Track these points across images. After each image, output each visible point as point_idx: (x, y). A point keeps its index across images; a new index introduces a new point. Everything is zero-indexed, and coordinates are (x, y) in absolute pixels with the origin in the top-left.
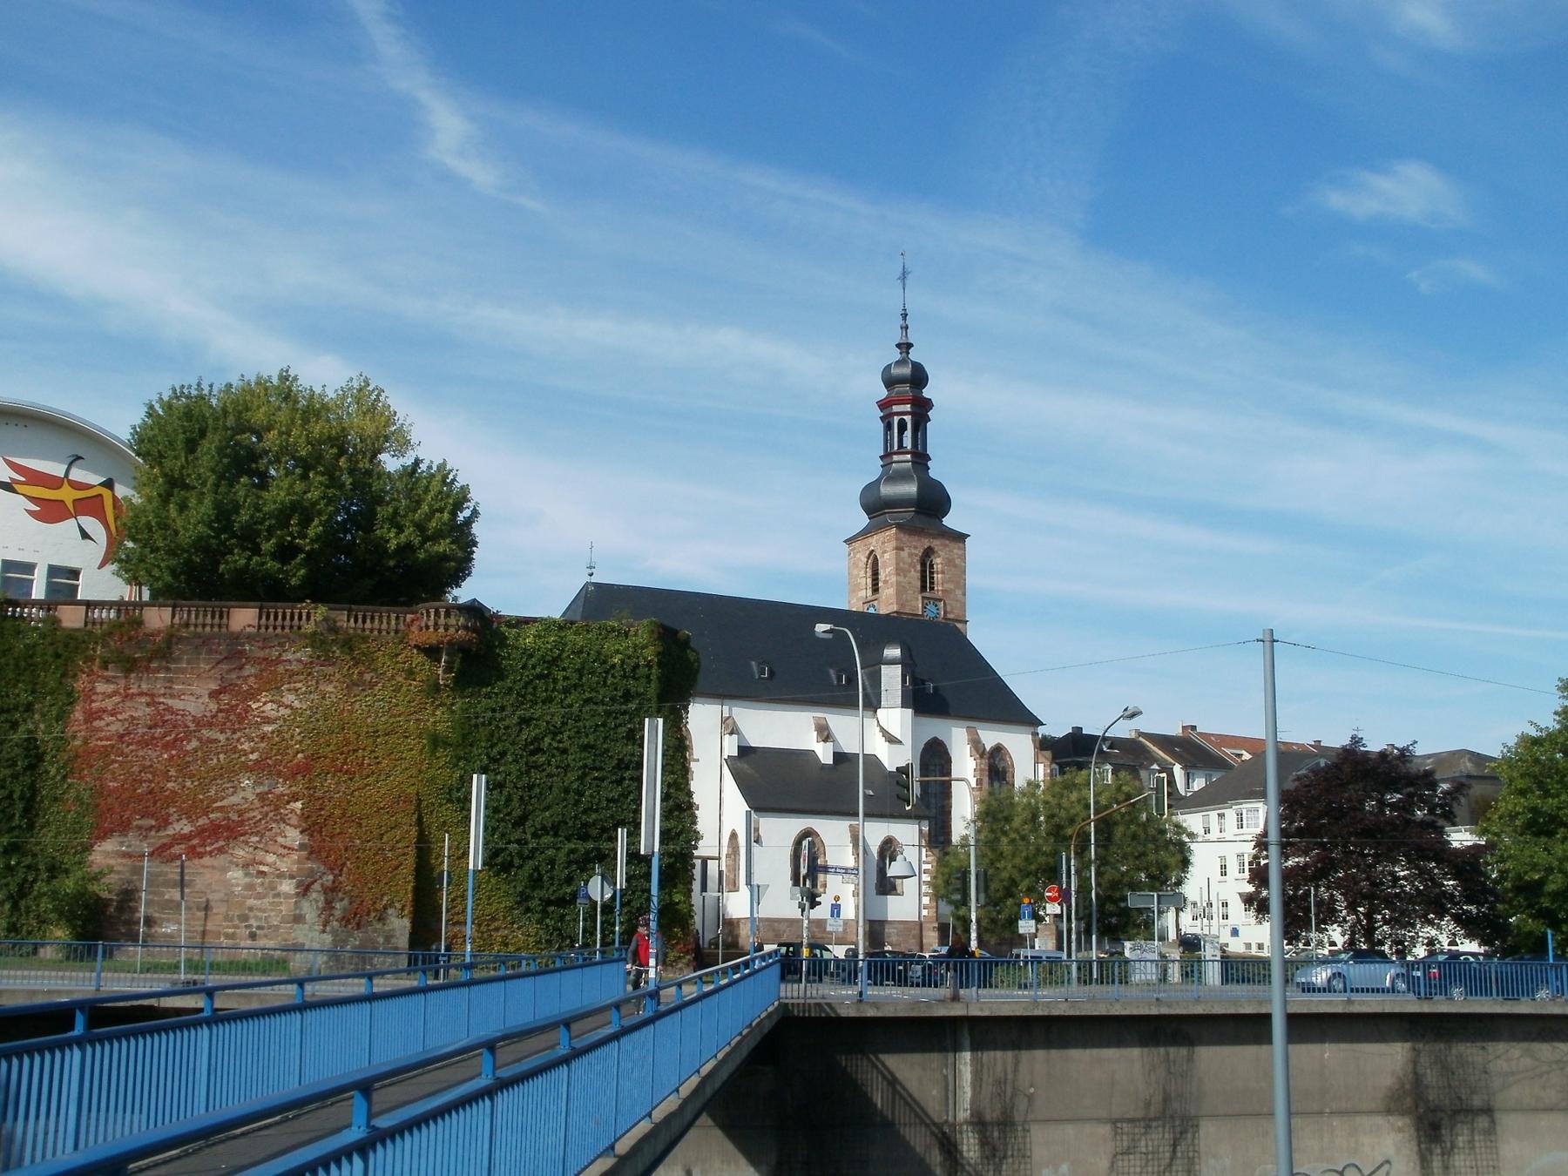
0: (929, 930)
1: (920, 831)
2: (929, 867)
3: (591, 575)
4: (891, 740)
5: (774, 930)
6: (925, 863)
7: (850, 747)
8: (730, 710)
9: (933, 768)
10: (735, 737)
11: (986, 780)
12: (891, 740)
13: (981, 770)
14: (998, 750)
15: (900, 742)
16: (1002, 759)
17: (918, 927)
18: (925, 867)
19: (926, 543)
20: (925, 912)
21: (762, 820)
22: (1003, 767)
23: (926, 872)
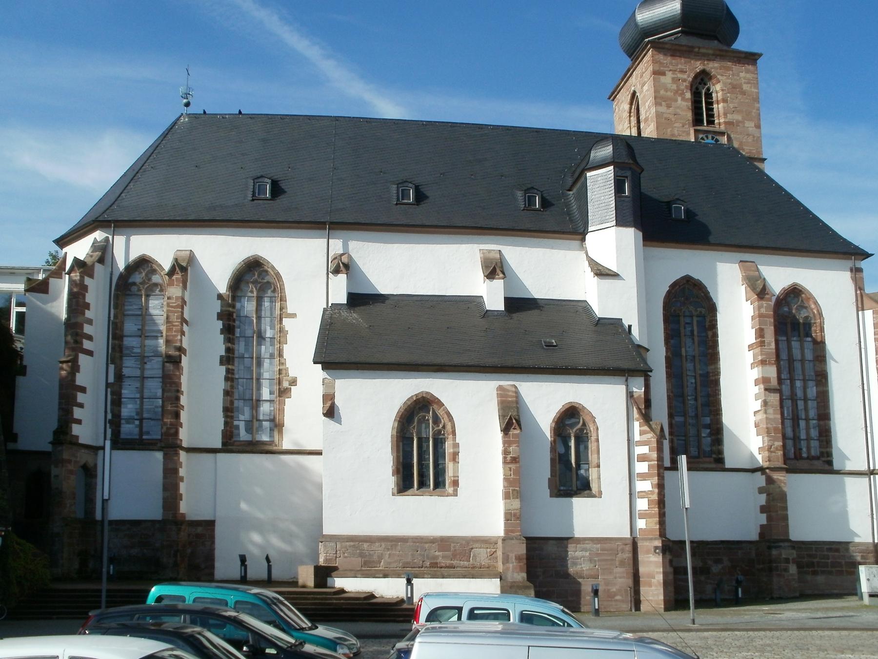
0: (648, 552)
1: (630, 395)
2: (644, 450)
3: (187, 105)
4: (602, 273)
5: (361, 555)
6: (641, 443)
7: (538, 289)
8: (345, 246)
9: (688, 320)
10: (342, 277)
11: (770, 331)
12: (602, 273)
13: (761, 316)
14: (794, 293)
15: (615, 275)
16: (803, 307)
17: (629, 548)
18: (640, 450)
19: (698, 66)
20: (641, 524)
21: (338, 382)
22: (807, 317)
23: (642, 458)
